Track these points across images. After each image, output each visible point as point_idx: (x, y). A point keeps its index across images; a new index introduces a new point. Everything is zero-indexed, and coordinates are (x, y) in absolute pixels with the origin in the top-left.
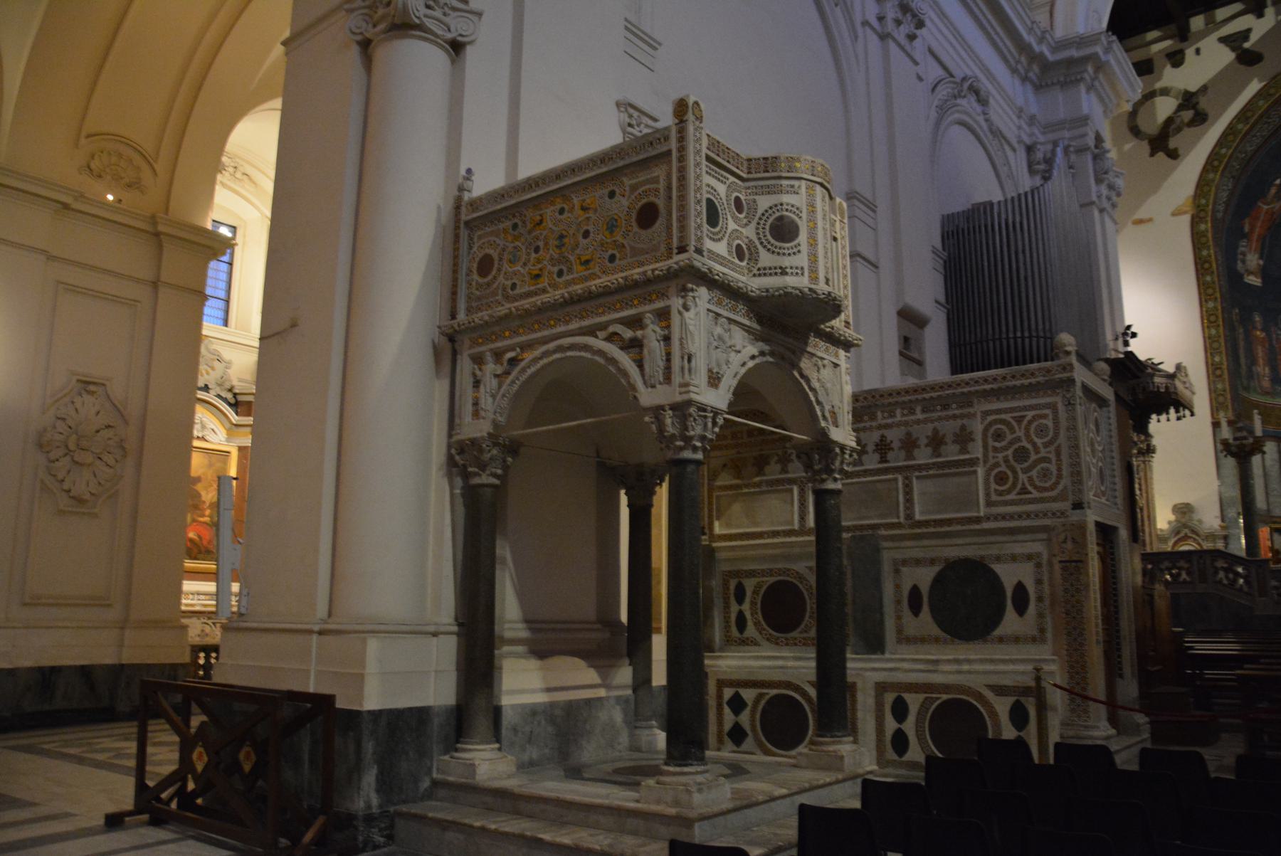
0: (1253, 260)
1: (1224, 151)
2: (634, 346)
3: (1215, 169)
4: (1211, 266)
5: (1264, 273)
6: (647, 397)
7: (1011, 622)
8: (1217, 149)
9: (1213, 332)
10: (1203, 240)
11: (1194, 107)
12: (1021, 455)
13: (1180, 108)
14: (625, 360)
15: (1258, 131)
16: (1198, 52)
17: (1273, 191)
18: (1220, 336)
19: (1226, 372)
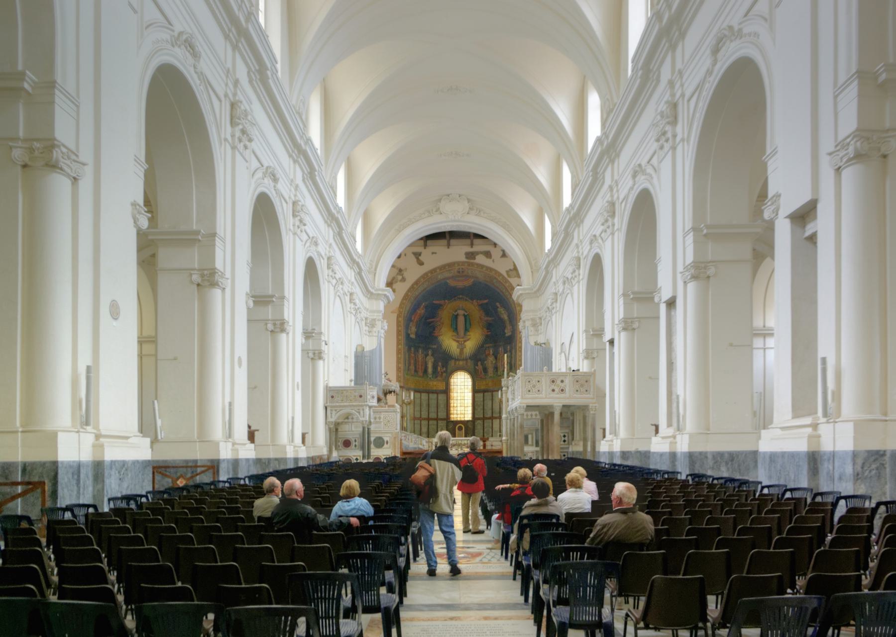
0: (413, 329)
2: (359, 413)
5: (416, 334)
6: (361, 419)
7: (385, 445)
9: (400, 356)
11: (402, 275)
12: (389, 421)
13: (398, 274)
14: (357, 414)
16: (405, 255)
17: (422, 307)
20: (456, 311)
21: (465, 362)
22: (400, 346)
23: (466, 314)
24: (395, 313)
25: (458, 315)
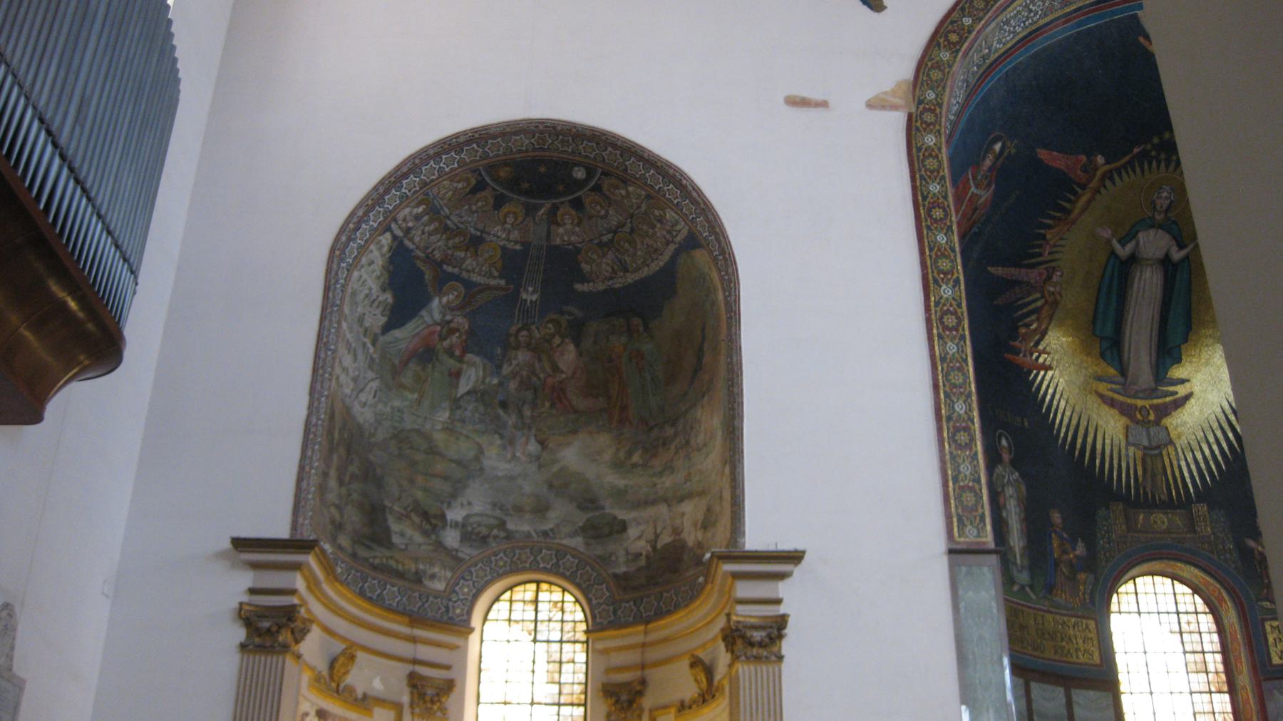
1: (967, 21)
3: (954, 48)
4: (946, 215)
8: (955, 14)
9: (952, 348)
10: (931, 163)
15: (1015, 16)
18: (966, 361)
19: (978, 435)
20: (1130, 236)
21: (1178, 520)
22: (946, 291)
23: (1177, 255)
24: (894, 107)
25: (1133, 259)
